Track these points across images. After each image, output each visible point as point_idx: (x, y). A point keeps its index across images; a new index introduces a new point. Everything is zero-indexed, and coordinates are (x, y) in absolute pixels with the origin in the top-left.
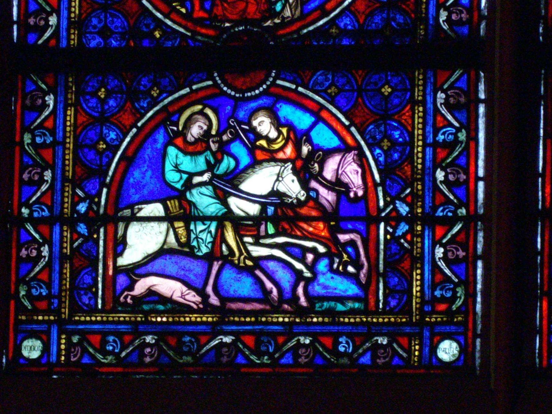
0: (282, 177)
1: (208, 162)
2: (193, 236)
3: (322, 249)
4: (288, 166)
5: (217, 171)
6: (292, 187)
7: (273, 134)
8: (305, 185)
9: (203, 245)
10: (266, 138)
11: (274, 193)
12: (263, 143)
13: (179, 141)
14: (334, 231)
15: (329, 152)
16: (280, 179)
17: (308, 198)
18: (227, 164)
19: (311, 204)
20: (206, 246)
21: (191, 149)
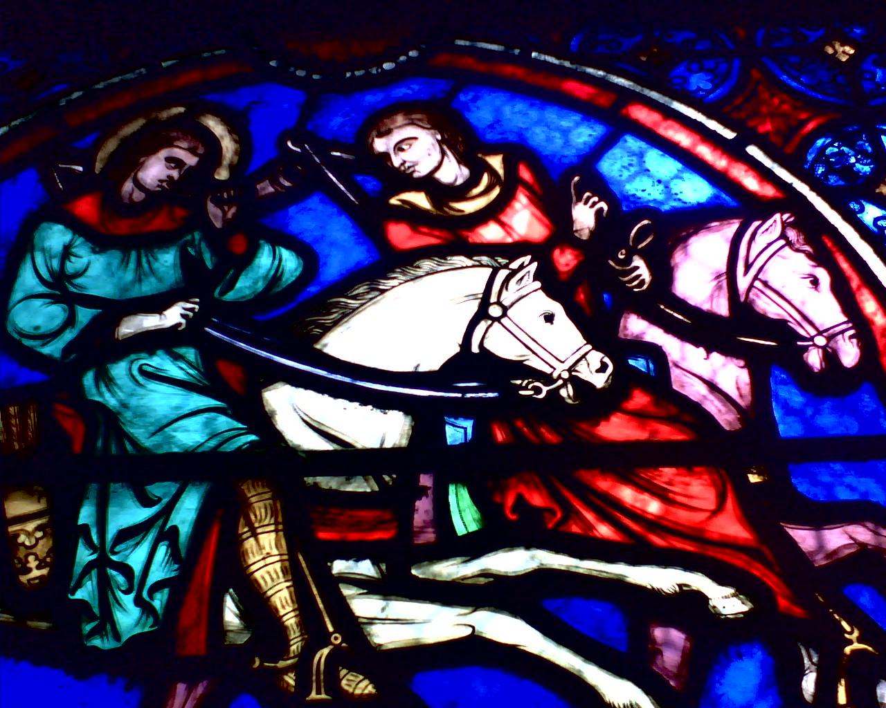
0: (499, 303)
1: (188, 264)
2: (84, 555)
3: (727, 602)
4: (522, 267)
5: (223, 293)
6: (544, 337)
7: (452, 172)
8: (598, 329)
9: (128, 600)
10: (429, 184)
11: (470, 363)
12: (420, 200)
13: (86, 207)
14: (769, 511)
15: (686, 223)
16: (495, 311)
17: (623, 380)
18: (275, 263)
19: (640, 399)
20: (138, 601)
21: (123, 227)
